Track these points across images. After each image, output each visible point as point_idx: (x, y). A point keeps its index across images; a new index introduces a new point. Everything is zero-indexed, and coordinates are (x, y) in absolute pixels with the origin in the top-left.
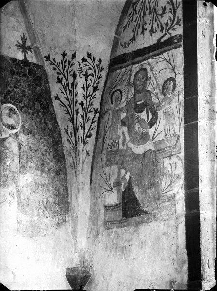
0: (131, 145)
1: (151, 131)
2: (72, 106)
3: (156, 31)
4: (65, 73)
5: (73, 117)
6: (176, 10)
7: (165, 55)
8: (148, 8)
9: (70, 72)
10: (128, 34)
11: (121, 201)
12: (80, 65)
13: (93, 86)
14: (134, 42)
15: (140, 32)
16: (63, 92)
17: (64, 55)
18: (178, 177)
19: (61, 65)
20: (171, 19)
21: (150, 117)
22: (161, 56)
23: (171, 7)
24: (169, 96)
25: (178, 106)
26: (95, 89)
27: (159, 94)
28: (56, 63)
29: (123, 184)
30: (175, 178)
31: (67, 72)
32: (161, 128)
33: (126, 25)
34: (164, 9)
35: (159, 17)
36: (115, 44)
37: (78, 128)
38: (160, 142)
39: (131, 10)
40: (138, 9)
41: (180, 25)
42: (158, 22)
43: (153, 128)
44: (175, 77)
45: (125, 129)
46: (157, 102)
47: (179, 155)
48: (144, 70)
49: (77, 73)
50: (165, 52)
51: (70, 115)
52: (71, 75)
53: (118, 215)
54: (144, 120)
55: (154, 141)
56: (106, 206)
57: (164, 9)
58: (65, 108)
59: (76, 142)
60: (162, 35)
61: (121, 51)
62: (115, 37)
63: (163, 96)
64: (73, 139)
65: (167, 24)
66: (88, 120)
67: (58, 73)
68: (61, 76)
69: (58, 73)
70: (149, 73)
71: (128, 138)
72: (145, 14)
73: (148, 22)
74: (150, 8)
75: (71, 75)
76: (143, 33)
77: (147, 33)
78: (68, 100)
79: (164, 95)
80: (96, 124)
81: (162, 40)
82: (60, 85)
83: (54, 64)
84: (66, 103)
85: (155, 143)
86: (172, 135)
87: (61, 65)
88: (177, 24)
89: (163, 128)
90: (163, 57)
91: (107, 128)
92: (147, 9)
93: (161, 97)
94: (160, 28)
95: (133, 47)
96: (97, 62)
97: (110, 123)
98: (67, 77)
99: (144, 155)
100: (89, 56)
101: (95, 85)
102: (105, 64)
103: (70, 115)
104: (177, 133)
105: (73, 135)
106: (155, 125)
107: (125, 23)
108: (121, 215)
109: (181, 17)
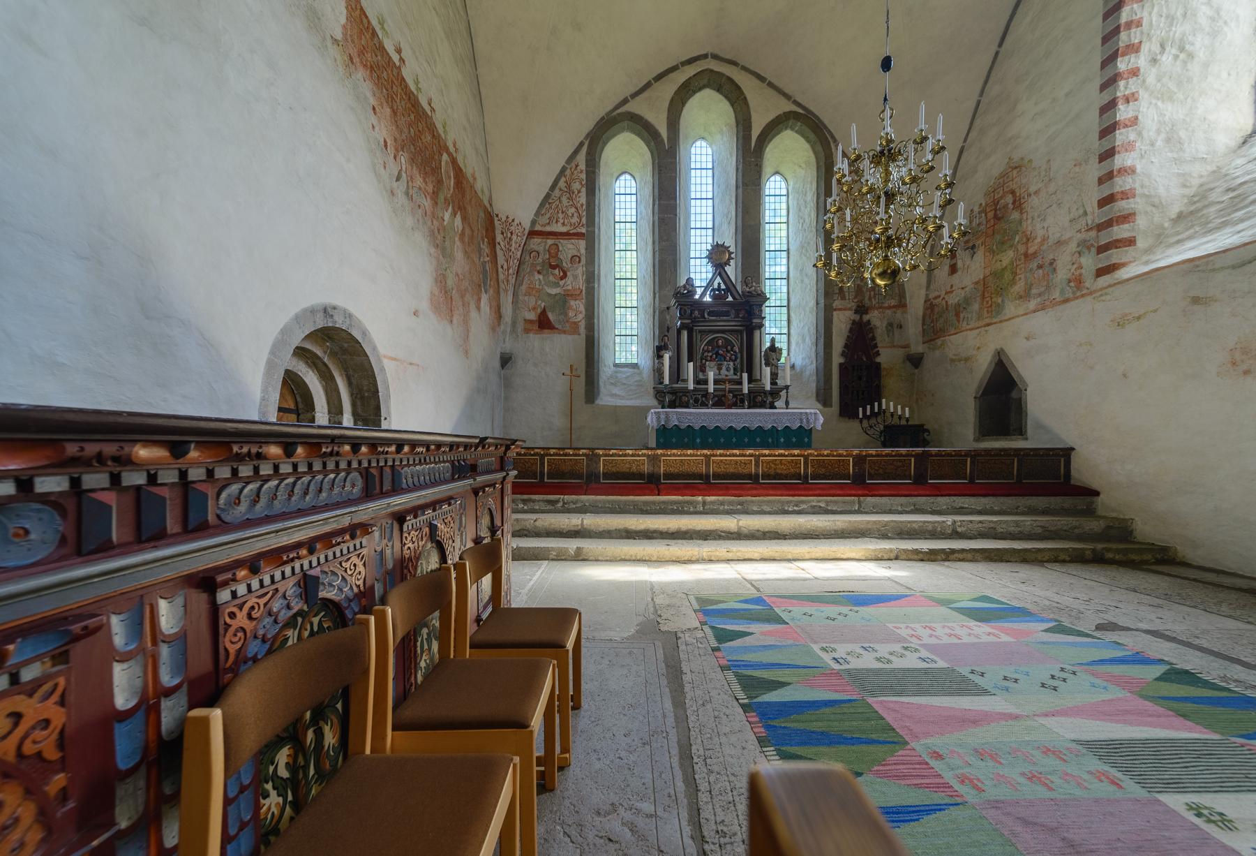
0: (546, 288)
1: (562, 283)
10: (544, 220)
21: (562, 274)
32: (569, 282)
34: (573, 215)
36: (534, 222)
38: (568, 290)
39: (547, 206)
43: (563, 281)
45: (541, 277)
48: (557, 245)
53: (536, 327)
56: (525, 320)
57: (573, 215)
61: (538, 228)
70: (561, 249)
71: (543, 283)
72: (558, 212)
76: (557, 222)
77: (559, 224)
81: (571, 232)
88: (582, 226)
93: (570, 265)
95: (548, 229)
97: (528, 270)
99: (555, 295)
102: (526, 232)
109: (584, 222)
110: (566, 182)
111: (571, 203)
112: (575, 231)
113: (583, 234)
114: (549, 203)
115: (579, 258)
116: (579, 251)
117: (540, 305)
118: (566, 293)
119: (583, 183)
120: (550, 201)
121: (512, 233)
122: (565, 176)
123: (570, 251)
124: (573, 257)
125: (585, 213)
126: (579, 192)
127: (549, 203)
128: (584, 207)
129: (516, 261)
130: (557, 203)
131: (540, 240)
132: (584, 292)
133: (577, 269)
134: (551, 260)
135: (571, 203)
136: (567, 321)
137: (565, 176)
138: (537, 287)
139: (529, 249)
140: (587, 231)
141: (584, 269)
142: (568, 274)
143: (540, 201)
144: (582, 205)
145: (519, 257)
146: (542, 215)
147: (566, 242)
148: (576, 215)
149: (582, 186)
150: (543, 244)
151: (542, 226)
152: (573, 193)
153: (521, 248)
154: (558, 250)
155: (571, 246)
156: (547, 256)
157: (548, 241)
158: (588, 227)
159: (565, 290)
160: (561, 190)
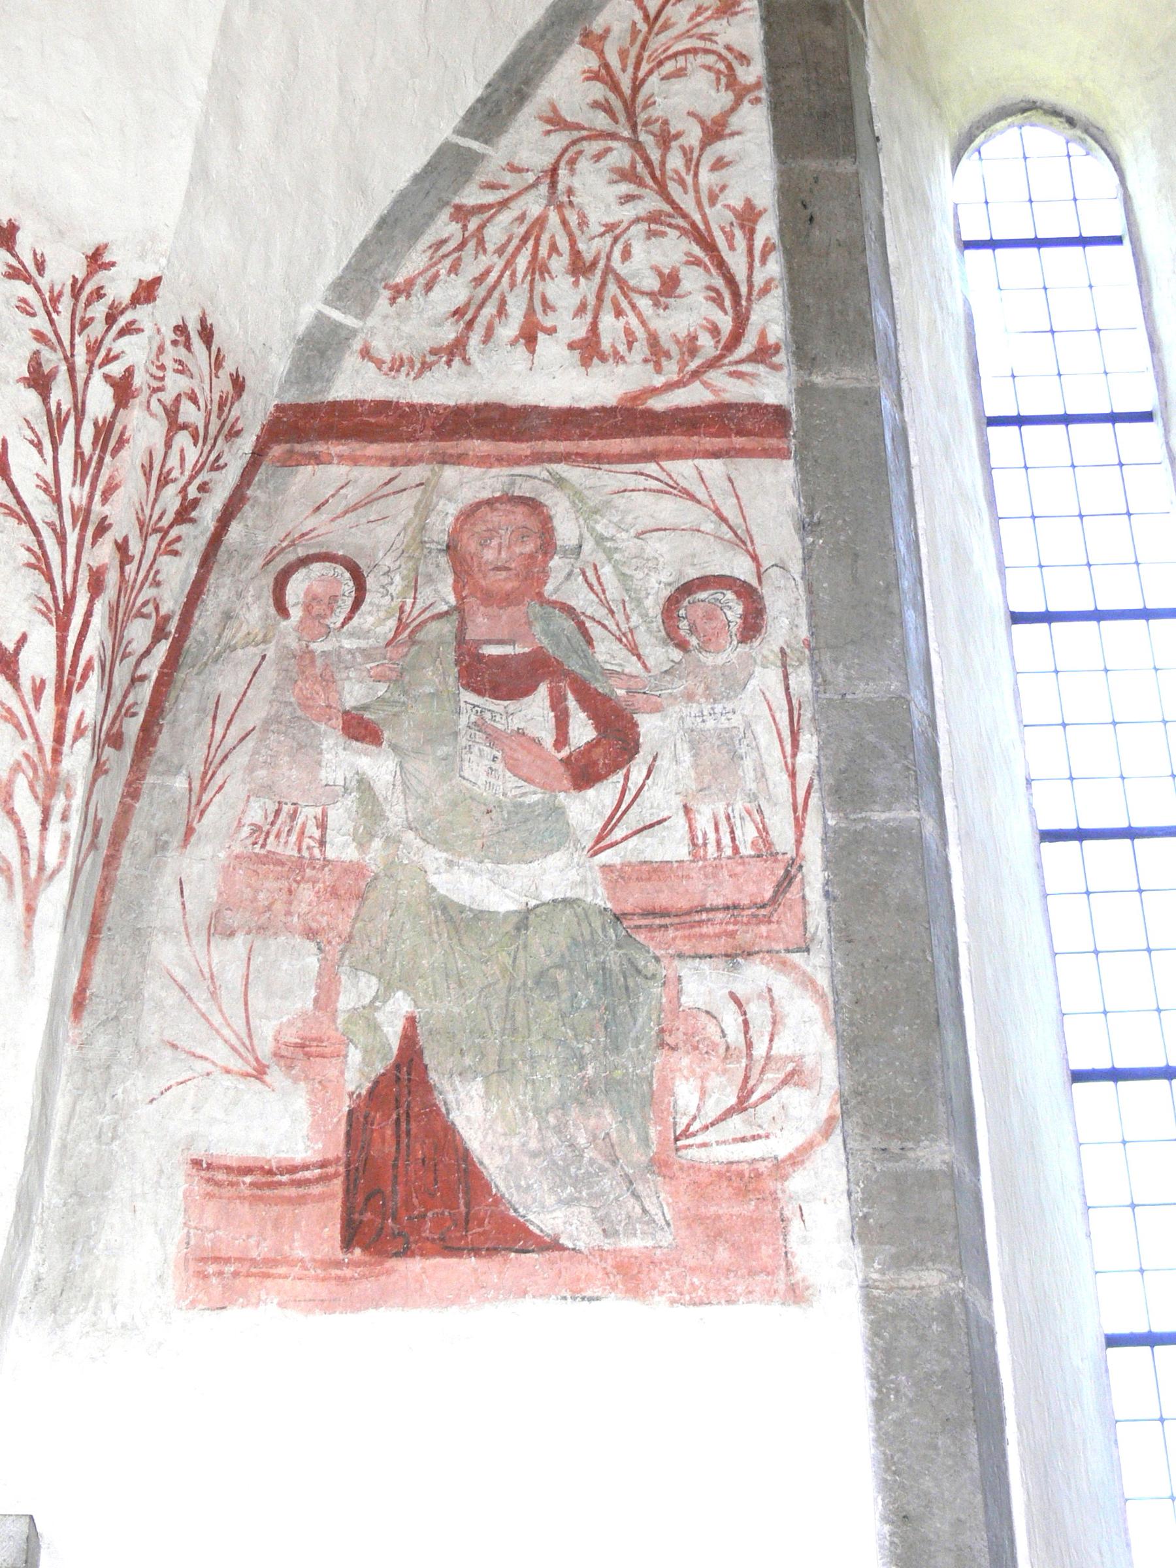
0: (433, 858)
2: (72, 538)
3: (619, 358)
4: (80, 360)
5: (70, 601)
6: (749, 299)
7: (683, 470)
8: (563, 244)
9: (108, 360)
11: (337, 1149)
12: (161, 350)
13: (184, 490)
14: (457, 362)
15: (509, 330)
16: (38, 446)
17: (96, 260)
18: (795, 1076)
19: (65, 305)
20: (715, 331)
21: (582, 731)
22: (651, 468)
23: (719, 283)
24: (708, 659)
25: (783, 718)
26: (184, 514)
27: (643, 638)
28: (43, 283)
29: (355, 1056)
30: (774, 1076)
31: (93, 349)
33: (410, 282)
34: (670, 284)
35: (644, 303)
37: (89, 666)
38: (656, 871)
39: (445, 227)
40: (495, 234)
41: (776, 368)
42: (634, 322)
43: (604, 795)
44: (754, 583)
46: (633, 666)
47: (797, 958)
48: (533, 505)
49: (139, 380)
50: (675, 454)
51: (50, 580)
52: (107, 377)
54: (537, 742)
55: (605, 857)
57: (670, 284)
58: (25, 531)
59: (59, 739)
60: (659, 381)
62: (319, 317)
63: (676, 654)
64: (45, 717)
65: (691, 346)
66: (124, 657)
67: (39, 336)
68: (51, 359)
69: (39, 336)
70: (566, 530)
71: (396, 812)
72: (538, 268)
73: (575, 301)
74: (576, 254)
75: (107, 377)
76: (529, 336)
78: (57, 500)
79: (682, 645)
80: (145, 691)
81: (658, 404)
82: (32, 397)
83: (28, 279)
84: (41, 508)
85: (606, 868)
86: (747, 850)
87: (65, 305)
88: (763, 353)
89: (677, 802)
90: (663, 476)
91: (235, 733)
92: (554, 248)
93: (659, 654)
94: (641, 349)
96: (224, 384)
98: (80, 383)
99: (524, 920)
100: (207, 334)
101: (192, 492)
103: (50, 580)
104: (783, 837)
105: (49, 692)
106: (619, 777)
107: (415, 261)
108: (333, 1231)
109: (777, 332)
110: (604, 75)
111: (651, 202)
112: (693, 396)
113: (779, 414)
114: (461, 214)
115: (748, 594)
116: (743, 541)
117: (366, 1016)
118: (635, 897)
119: (753, 72)
120: (471, 196)
121: (123, 390)
122: (594, 41)
123: (657, 546)
124: (687, 589)
125: (774, 267)
126: (715, 131)
127: (461, 214)
128: (767, 228)
129: (139, 632)
130: (534, 205)
131: (371, 476)
132: (815, 874)
133: (734, 683)
134: (480, 624)
135: (651, 202)
136: (660, 1165)
137: (594, 41)
138: (340, 848)
139: (267, 540)
140: (804, 391)
141: (802, 681)
142: (649, 726)
143: (382, 203)
144: (748, 217)
145: (171, 601)
146: (401, 291)
147: (609, 478)
148: (693, 281)
149: (741, 94)
150: (407, 501)
151: (397, 365)
152: (666, 139)
153: (195, 537)
154: (548, 545)
155: (669, 509)
156: (443, 592)
157: (450, 474)
158: (804, 358)
159: (616, 877)
160: (555, 121)
